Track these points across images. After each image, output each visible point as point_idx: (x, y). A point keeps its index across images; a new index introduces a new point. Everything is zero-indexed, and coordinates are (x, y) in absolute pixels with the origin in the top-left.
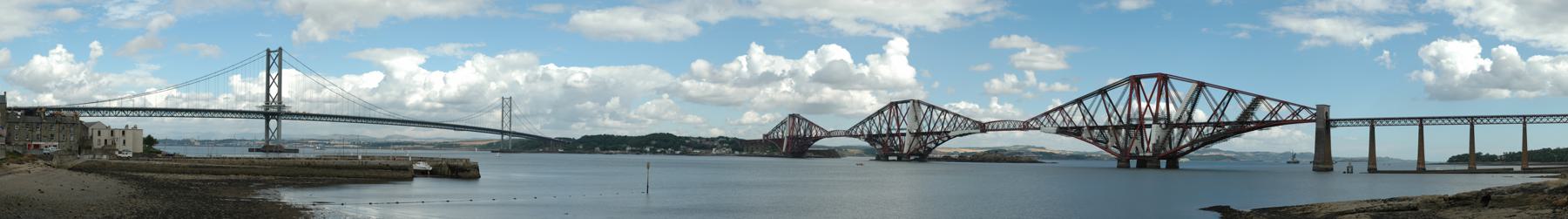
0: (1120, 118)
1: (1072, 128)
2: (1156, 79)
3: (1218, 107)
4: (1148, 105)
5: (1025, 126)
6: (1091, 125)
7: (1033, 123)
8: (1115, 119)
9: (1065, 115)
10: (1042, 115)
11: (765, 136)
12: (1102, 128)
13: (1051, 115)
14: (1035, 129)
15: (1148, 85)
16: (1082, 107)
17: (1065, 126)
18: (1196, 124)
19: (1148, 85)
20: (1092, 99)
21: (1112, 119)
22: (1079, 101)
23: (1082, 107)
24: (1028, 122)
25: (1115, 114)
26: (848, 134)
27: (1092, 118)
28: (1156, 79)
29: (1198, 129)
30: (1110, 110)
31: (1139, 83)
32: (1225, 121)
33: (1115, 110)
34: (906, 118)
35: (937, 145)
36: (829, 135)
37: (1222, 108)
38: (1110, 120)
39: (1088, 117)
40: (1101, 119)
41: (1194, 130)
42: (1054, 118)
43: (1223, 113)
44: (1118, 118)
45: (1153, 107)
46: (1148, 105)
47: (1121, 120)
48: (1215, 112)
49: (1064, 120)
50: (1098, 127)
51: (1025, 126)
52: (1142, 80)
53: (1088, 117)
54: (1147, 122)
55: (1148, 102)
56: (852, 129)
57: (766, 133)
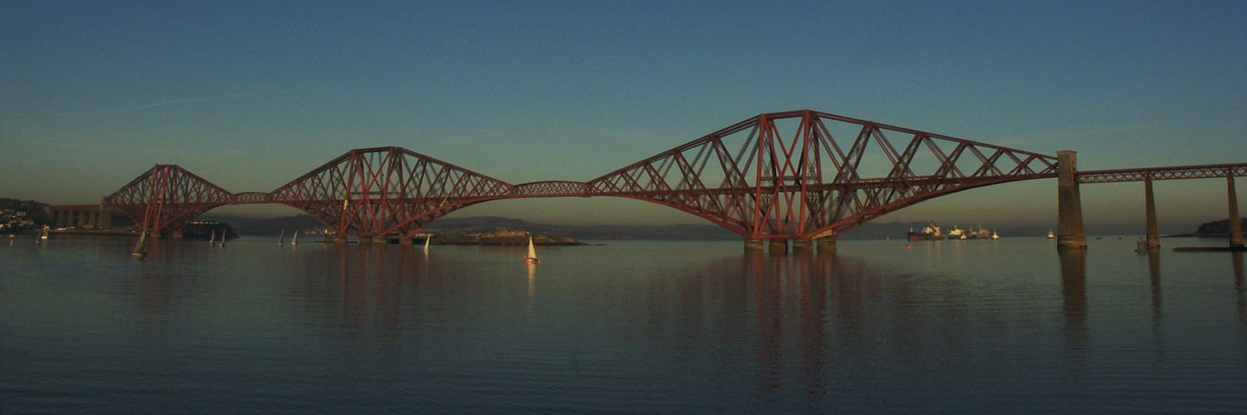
0: (742, 176)
3: (901, 159)
4: (788, 162)
5: (588, 189)
6: (695, 187)
7: (602, 186)
8: (735, 178)
9: (653, 174)
12: (715, 193)
13: (630, 173)
14: (602, 194)
15: (788, 130)
16: (681, 161)
19: (788, 130)
21: (732, 180)
22: (677, 152)
23: (681, 161)
24: (591, 184)
27: (696, 177)
28: (800, 119)
29: (868, 193)
30: (729, 166)
33: (734, 166)
38: (728, 180)
41: (861, 194)
44: (739, 177)
45: (795, 159)
46: (788, 162)
47: (743, 181)
48: (896, 166)
49: (653, 181)
50: (706, 191)
53: (691, 175)
54: (788, 183)
55: (788, 157)
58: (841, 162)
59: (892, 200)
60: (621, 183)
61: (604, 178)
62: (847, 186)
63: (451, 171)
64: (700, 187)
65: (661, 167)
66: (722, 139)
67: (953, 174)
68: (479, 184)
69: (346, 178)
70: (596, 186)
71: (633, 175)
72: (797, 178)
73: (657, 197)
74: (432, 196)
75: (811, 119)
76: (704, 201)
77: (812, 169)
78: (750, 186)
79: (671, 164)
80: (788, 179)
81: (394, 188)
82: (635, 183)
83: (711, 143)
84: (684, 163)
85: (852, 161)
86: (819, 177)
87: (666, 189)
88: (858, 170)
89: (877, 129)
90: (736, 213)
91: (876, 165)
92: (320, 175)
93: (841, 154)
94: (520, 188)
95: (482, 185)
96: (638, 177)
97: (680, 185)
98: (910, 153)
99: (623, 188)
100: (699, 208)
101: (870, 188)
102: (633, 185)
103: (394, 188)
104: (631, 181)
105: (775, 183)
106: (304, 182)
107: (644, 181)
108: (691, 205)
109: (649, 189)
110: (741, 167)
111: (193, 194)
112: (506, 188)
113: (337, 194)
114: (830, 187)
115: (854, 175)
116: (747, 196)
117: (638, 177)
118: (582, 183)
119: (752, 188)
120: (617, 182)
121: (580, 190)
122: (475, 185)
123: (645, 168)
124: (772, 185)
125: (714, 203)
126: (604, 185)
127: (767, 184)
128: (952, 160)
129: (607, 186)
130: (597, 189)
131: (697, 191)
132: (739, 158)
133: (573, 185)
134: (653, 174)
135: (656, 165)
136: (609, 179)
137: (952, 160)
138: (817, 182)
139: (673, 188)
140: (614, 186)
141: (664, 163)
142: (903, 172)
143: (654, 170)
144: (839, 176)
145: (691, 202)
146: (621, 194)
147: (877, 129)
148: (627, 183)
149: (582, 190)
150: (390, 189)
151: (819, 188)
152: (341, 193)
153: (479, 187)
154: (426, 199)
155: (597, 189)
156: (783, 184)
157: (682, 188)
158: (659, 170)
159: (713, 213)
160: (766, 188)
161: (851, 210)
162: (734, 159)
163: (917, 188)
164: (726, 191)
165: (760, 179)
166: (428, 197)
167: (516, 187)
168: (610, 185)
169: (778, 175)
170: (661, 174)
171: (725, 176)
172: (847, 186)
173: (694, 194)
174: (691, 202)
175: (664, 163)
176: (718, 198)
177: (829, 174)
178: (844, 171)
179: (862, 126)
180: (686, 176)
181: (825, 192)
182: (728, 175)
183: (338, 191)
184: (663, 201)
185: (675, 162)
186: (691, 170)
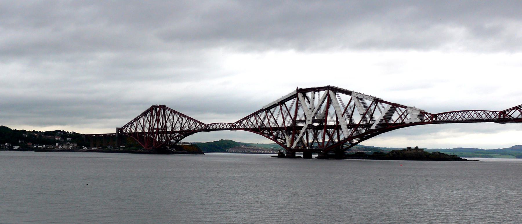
11: (118, 129)
24: (504, 113)
36: (207, 129)
63: (379, 104)
68: (403, 114)
69: (293, 113)
70: (510, 114)
74: (364, 123)
81: (332, 118)
92: (272, 110)
94: (439, 117)
95: (406, 114)
103: (332, 118)
106: (259, 115)
111: (178, 125)
112: (427, 117)
113: (286, 123)
121: (495, 117)
122: (401, 114)
130: (510, 116)
133: (488, 114)
150: (329, 119)
152: (289, 122)
153: (403, 116)
154: (359, 125)
166: (360, 124)
167: (436, 116)
183: (287, 121)
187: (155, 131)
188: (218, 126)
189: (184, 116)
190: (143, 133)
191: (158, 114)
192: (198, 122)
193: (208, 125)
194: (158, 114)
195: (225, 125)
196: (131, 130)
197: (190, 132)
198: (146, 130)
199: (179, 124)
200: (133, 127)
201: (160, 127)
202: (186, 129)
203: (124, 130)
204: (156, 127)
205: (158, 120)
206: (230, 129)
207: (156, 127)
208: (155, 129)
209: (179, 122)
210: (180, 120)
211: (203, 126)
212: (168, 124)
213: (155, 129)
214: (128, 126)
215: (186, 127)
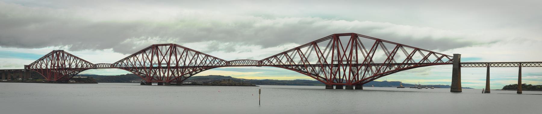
1: (293, 65)
2: (350, 37)
3: (390, 55)
4: (345, 54)
5: (260, 64)
6: (306, 64)
9: (288, 57)
10: (272, 57)
11: (26, 66)
12: (314, 66)
13: (278, 57)
14: (266, 65)
15: (345, 40)
16: (300, 52)
17: (289, 63)
18: (374, 65)
19: (345, 40)
20: (307, 48)
21: (321, 60)
23: (300, 52)
24: (261, 61)
25: (322, 58)
26: (113, 66)
28: (350, 37)
29: (377, 68)
30: (320, 55)
31: (338, 39)
32: (394, 62)
33: (322, 55)
34: (165, 58)
35: (191, 75)
37: (392, 55)
38: (319, 61)
39: (304, 59)
40: (314, 61)
42: (280, 59)
43: (392, 58)
44: (324, 60)
45: (348, 53)
47: (325, 61)
48: (388, 58)
49: (288, 60)
50: (310, 65)
51: (260, 64)
52: (340, 37)
53: (304, 59)
56: (117, 63)
57: (28, 64)
58: (366, 55)
59: (386, 71)
60: (274, 61)
61: (267, 59)
62: (368, 64)
64: (308, 64)
65: (292, 55)
66: (317, 44)
67: (411, 61)
70: (264, 62)
71: (280, 58)
72: (348, 60)
73: (290, 67)
75: (354, 37)
76: (309, 69)
77: (354, 58)
78: (328, 63)
79: (296, 54)
80: (344, 61)
82: (280, 61)
83: (313, 45)
84: (301, 54)
85: (371, 55)
86: (357, 61)
87: (293, 64)
88: (373, 59)
89: (381, 42)
90: (322, 74)
91: (380, 56)
93: (366, 52)
96: (282, 59)
97: (299, 63)
98: (394, 53)
99: (275, 63)
100: (307, 72)
101: (378, 66)
102: (280, 62)
104: (279, 60)
105: (339, 62)
107: (284, 61)
108: (304, 71)
109: (286, 64)
110: (325, 56)
114: (361, 65)
115: (371, 60)
116: (327, 68)
117: (282, 59)
118: (257, 61)
119: (329, 65)
120: (273, 61)
121: (257, 64)
123: (285, 55)
124: (338, 63)
125: (313, 70)
126: (267, 62)
127: (336, 63)
128: (411, 56)
129: (269, 62)
130: (264, 63)
131: (307, 65)
132: (324, 52)
133: (254, 62)
134: (288, 57)
135: (289, 54)
136: (270, 59)
137: (411, 56)
138: (356, 63)
139: (297, 63)
140: (271, 62)
141: (293, 53)
142: (391, 60)
143: (289, 56)
144: (366, 60)
145: (304, 69)
146: (274, 66)
147: (381, 42)
148: (277, 61)
149: (258, 64)
151: (357, 65)
155: (264, 63)
156: (342, 63)
157: (300, 64)
158: (291, 56)
159: (313, 74)
160: (335, 65)
161: (369, 75)
162: (322, 52)
163: (396, 66)
164: (318, 65)
165: (333, 61)
168: (270, 62)
169: (340, 59)
170: (292, 57)
171: (318, 59)
172: (368, 64)
173: (306, 66)
174: (304, 69)
175: (293, 53)
176: (315, 68)
177: (361, 58)
178: (367, 58)
179: (375, 41)
180: (302, 59)
181: (359, 67)
182: (319, 59)
184: (292, 69)
185: (298, 53)
186: (304, 56)
187: (56, 68)
188: (102, 65)
189: (78, 58)
190: (47, 69)
191: (58, 56)
192: (88, 62)
193: (95, 65)
194: (58, 56)
195: (107, 65)
196: (36, 66)
197: (83, 69)
198: (49, 67)
199: (74, 63)
200: (38, 65)
201: (60, 65)
202: (80, 67)
203: (31, 67)
204: (56, 65)
205: (58, 59)
206: (111, 68)
207: (56, 65)
208: (56, 67)
209: (74, 62)
210: (75, 61)
211: (92, 65)
212: (66, 63)
213: (56, 67)
214: (34, 64)
215: (79, 66)
